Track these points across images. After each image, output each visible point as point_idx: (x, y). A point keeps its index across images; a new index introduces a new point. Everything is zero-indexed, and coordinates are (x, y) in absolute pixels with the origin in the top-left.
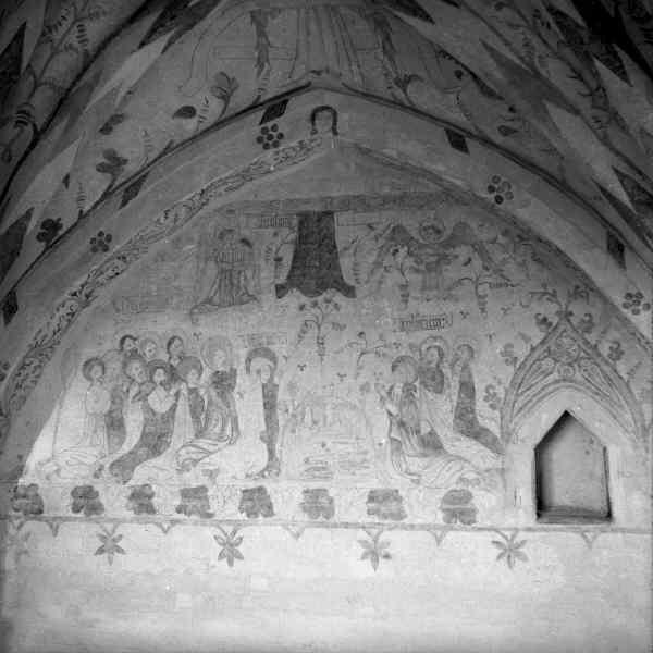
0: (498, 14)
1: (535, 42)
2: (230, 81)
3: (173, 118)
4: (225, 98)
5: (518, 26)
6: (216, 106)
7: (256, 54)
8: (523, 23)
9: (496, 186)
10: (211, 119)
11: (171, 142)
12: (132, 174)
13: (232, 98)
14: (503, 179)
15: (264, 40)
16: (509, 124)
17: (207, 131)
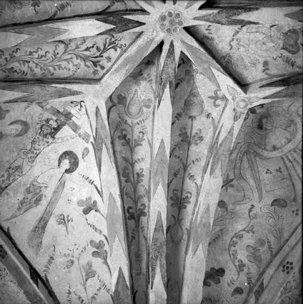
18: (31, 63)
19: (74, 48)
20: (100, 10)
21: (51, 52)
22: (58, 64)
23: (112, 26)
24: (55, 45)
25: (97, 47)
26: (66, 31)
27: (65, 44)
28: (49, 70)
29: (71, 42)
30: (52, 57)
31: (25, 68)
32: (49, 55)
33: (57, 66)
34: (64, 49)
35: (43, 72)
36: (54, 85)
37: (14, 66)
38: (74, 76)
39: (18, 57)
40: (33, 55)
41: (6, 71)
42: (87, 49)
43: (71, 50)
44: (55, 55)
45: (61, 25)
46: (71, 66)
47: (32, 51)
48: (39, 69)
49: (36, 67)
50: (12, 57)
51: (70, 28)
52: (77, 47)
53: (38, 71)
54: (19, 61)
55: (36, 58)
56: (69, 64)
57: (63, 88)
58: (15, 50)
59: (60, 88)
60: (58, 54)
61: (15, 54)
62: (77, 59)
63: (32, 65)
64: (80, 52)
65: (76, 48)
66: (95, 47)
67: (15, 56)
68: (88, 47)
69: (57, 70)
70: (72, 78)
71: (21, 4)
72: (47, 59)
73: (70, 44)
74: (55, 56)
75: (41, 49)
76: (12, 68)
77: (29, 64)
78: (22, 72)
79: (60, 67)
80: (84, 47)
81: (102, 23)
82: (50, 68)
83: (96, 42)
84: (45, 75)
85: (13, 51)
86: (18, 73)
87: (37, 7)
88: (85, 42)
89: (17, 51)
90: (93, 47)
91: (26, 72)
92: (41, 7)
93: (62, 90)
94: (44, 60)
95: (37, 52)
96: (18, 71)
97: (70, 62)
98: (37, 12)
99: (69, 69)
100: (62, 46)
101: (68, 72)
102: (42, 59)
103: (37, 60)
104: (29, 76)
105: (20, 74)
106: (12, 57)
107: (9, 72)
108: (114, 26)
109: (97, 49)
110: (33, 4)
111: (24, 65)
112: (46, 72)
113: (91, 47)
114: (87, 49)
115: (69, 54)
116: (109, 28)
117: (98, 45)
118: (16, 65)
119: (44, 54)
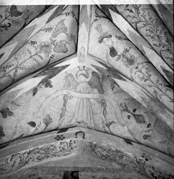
0: (145, 83)
1: (157, 90)
2: (50, 119)
3: (28, 124)
4: (47, 124)
5: (152, 86)
6: (43, 126)
7: (61, 112)
8: (153, 85)
9: (145, 156)
10: (40, 130)
11: (23, 135)
12: (4, 142)
13: (49, 125)
14: (147, 154)
15: (65, 108)
16: (147, 134)
17: (37, 134)
18: (157, 34)
19: (135, 18)
20: (108, 20)
21: (145, 28)
22: (149, 20)
23: (110, 10)
24: (140, 29)
25: (126, 7)
26: (128, 31)
27: (136, 25)
28: (156, 22)
29: (133, 22)
30: (148, 26)
31: (163, 35)
32: (148, 28)
33: (150, 20)
34: (140, 23)
35: (158, 25)
36: (161, 17)
37: (165, 41)
38: (150, 8)
39: (159, 42)
40: (153, 36)
41: (169, 44)
42: (131, 11)
43: (138, 19)
44: (145, 25)
45: (127, 34)
46: (147, 12)
47: (150, 38)
48: (158, 28)
49: (158, 30)
50: (160, 45)
51: (126, 30)
52: (134, 17)
53: (160, 28)
54: (160, 41)
55: (153, 33)
56: (145, 15)
57: (160, 11)
58: (156, 46)
59: (161, 13)
60: (144, 24)
61: (158, 45)
62: (140, 13)
63: (158, 33)
64: (135, 13)
65: (135, 17)
66: (127, 8)
67: (159, 44)
68: (130, 12)
69: (153, 19)
70: (152, 8)
71: (131, 57)
72: (150, 27)
73: (134, 22)
74: (146, 25)
75: (147, 34)
76: (166, 41)
77: (159, 34)
78: (166, 35)
79: (150, 19)
80: (132, 14)
81: (112, 17)
82: (154, 23)
83: (125, 10)
84: (160, 23)
85: (157, 46)
86: (168, 37)
87: (128, 50)
88: (128, 15)
89: (156, 45)
90: (128, 9)
91: (165, 34)
92: (127, 48)
93: (161, 11)
94: (152, 29)
95: (150, 35)
96: (166, 37)
97: (144, 15)
98: (130, 48)
99: (148, 13)
100: (139, 25)
101: (150, 13)
102: (152, 30)
103: (154, 32)
104: (166, 30)
105: (168, 36)
106: (160, 45)
107: (169, 42)
108: (109, 9)
109: (128, 6)
110: (128, 52)
111: (161, 37)
112: (158, 24)
113: (129, 10)
114: (131, 11)
115: (140, 19)
116: (112, 11)
117: (125, 8)
118: (164, 41)
119: (149, 31)
